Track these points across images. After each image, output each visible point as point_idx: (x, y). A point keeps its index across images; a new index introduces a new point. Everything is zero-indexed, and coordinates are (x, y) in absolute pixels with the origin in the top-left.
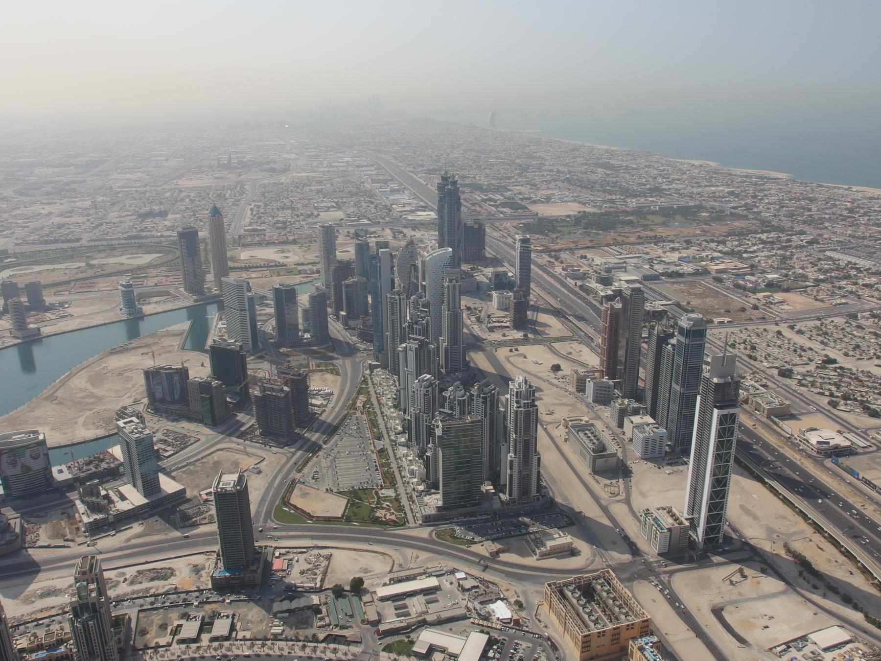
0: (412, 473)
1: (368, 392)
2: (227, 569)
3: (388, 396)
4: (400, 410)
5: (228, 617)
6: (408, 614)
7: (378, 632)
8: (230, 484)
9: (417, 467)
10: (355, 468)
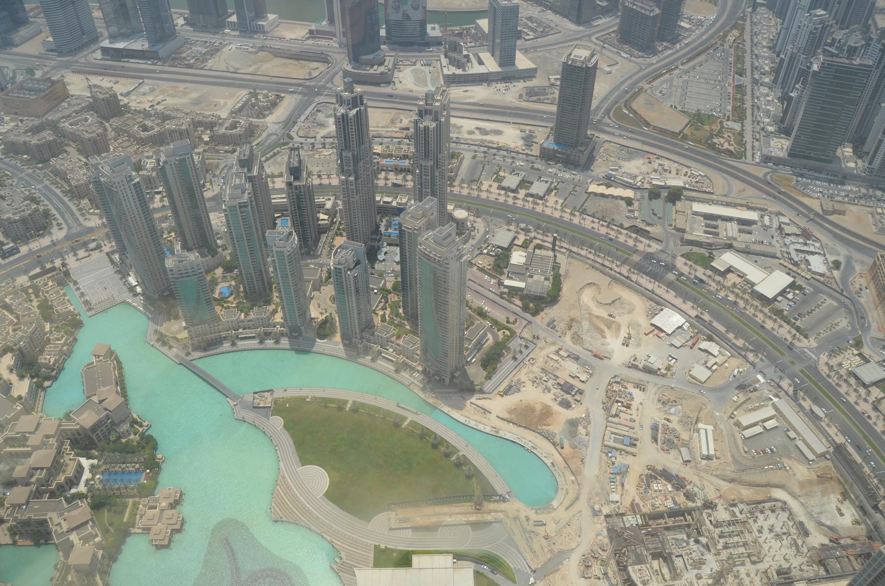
0: (768, 113)
1: (744, 29)
2: (557, 142)
3: (765, 36)
4: (773, 53)
5: (547, 182)
6: (717, 234)
7: (682, 239)
8: (581, 57)
9: (775, 108)
10: (705, 94)
